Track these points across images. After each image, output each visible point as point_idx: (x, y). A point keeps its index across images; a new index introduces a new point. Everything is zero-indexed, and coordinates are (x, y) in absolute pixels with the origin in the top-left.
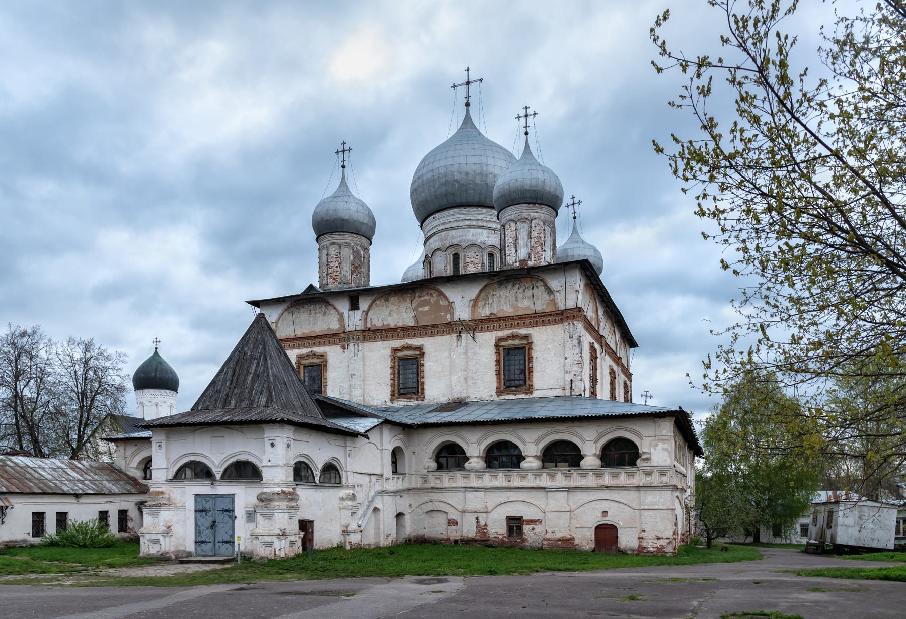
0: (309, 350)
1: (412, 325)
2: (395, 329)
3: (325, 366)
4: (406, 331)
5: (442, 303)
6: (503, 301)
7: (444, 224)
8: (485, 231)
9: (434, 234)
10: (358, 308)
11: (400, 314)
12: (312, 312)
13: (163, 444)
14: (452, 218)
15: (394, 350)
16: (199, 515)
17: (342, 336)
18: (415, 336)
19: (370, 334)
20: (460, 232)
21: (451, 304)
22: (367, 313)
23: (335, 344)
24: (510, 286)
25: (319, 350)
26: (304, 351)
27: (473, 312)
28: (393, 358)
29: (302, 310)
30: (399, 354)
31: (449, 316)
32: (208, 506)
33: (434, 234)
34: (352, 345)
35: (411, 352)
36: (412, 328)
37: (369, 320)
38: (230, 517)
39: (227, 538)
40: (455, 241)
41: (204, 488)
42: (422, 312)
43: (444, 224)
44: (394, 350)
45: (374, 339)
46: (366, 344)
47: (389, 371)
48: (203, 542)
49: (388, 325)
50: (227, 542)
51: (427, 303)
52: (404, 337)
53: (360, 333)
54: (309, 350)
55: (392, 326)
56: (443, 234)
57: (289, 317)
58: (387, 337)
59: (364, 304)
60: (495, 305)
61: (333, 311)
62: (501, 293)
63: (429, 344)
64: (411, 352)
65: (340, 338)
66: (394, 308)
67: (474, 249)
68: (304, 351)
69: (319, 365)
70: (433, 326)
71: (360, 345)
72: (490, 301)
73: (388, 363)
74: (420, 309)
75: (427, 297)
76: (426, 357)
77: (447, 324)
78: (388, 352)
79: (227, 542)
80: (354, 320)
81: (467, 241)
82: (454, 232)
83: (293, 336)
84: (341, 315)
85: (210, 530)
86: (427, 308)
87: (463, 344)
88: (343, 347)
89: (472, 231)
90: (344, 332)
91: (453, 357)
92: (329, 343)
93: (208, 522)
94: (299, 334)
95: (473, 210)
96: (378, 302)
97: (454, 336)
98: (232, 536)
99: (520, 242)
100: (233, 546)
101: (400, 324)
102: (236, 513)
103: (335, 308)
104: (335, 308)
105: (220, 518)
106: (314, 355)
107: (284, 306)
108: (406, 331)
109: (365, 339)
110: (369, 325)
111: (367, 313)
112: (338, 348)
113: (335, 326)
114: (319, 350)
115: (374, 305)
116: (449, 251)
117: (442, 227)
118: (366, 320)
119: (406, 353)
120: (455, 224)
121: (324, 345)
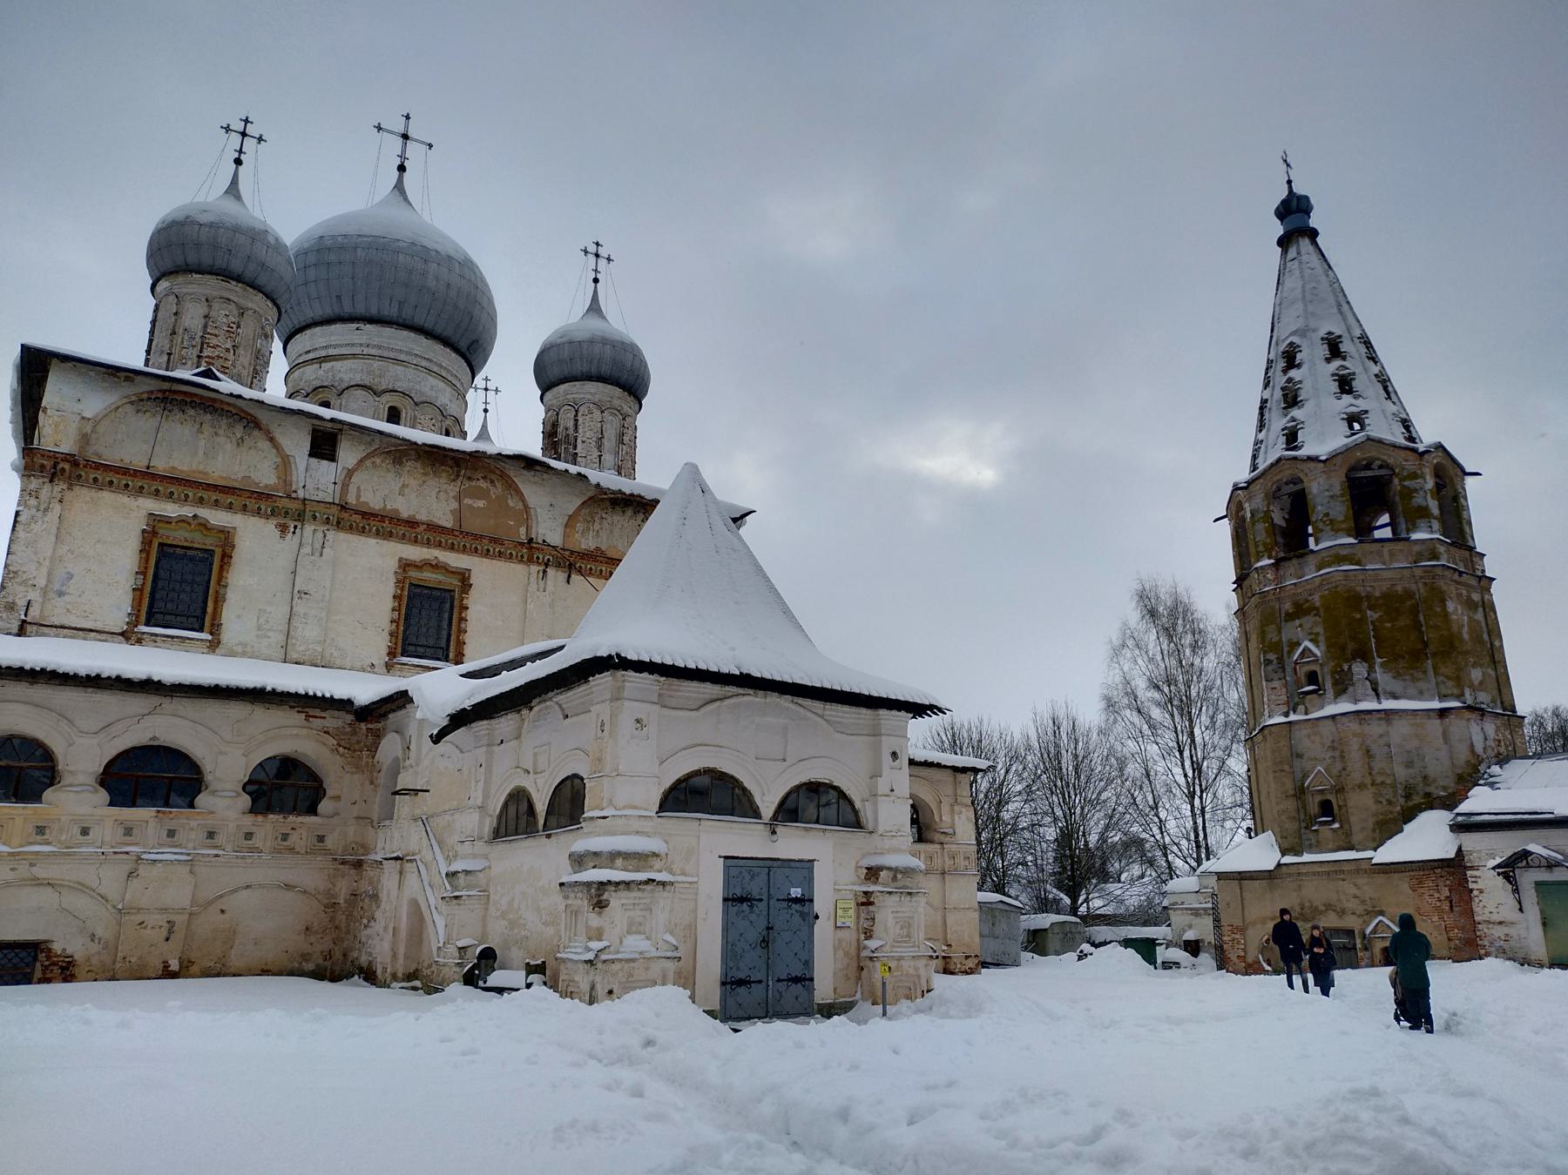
0: (188, 511)
1: (449, 525)
2: (412, 523)
3: (226, 557)
4: (432, 533)
5: (511, 503)
6: (616, 531)
7: (380, 347)
8: (448, 389)
9: (354, 356)
10: (332, 458)
11: (431, 500)
12: (207, 429)
13: (650, 712)
14: (399, 345)
15: (405, 565)
16: (733, 910)
17: (285, 503)
18: (452, 548)
19: (353, 518)
20: (411, 373)
21: (526, 507)
22: (350, 473)
23: (258, 512)
24: (629, 512)
25: (217, 518)
26: (171, 510)
27: (565, 536)
28: (399, 583)
29: (179, 415)
30: (413, 574)
31: (523, 530)
32: (756, 888)
33: (354, 356)
34: (309, 528)
35: (440, 577)
36: (450, 531)
37: (352, 489)
38: (803, 916)
39: (797, 972)
40: (400, 386)
41: (747, 840)
42: (470, 506)
43: (380, 347)
44: (405, 565)
45: (362, 531)
46: (342, 536)
47: (389, 603)
48: (741, 983)
49: (396, 511)
50: (796, 980)
51: (483, 494)
52: (428, 544)
53: (335, 510)
54: (188, 511)
55: (405, 515)
56: (376, 364)
57: (146, 423)
58: (391, 534)
59: (348, 454)
60: (603, 534)
61: (264, 444)
62: (616, 518)
63: (482, 570)
64: (440, 577)
65: (286, 509)
66: (413, 482)
67: (429, 409)
68: (171, 510)
69: (211, 553)
70: (494, 540)
71: (331, 535)
72: (597, 527)
73: (390, 589)
74: (467, 501)
75: (483, 484)
76: (473, 592)
77: (522, 544)
78: (392, 565)
79: (796, 980)
80: (318, 479)
81: (422, 394)
82: (400, 369)
83: (139, 463)
84: (285, 463)
85: (759, 951)
86: (481, 504)
87: (550, 588)
88: (283, 529)
89: (433, 381)
90: (289, 497)
91: (530, 606)
92: (244, 509)
93: (754, 935)
94: (161, 465)
95: (439, 347)
96: (378, 461)
97: (534, 568)
98: (808, 963)
99: (605, 441)
100: (811, 990)
101: (422, 516)
102: (818, 907)
103: (272, 439)
104: (272, 439)
105: (784, 918)
106: (204, 526)
107: (130, 390)
108: (432, 533)
109: (339, 525)
110: (351, 499)
111: (350, 473)
112: (269, 528)
113: (264, 474)
114: (217, 518)
115: (368, 463)
116: (386, 398)
117: (373, 352)
118: (345, 487)
119: (429, 577)
120: (402, 357)
121: (230, 507)
